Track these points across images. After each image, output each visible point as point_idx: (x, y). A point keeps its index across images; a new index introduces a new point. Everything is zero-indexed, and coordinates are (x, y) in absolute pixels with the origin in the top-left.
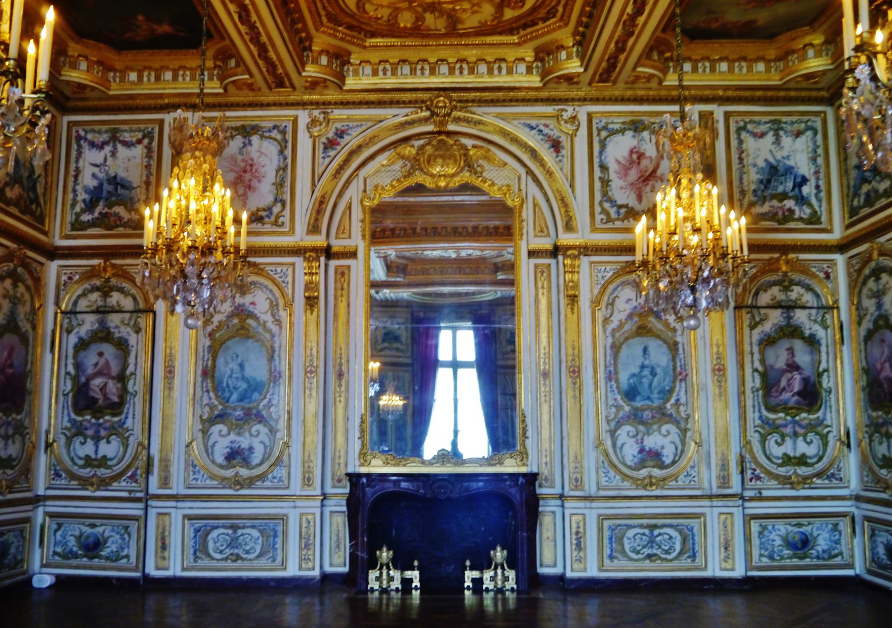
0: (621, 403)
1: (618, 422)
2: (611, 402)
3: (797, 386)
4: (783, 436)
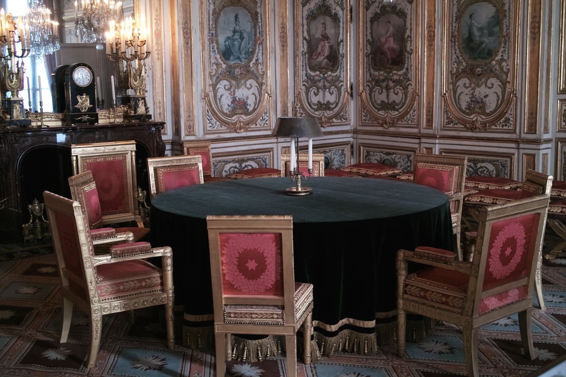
0: (220, 61)
1: (218, 77)
2: (213, 61)
3: (326, 53)
4: (318, 89)
